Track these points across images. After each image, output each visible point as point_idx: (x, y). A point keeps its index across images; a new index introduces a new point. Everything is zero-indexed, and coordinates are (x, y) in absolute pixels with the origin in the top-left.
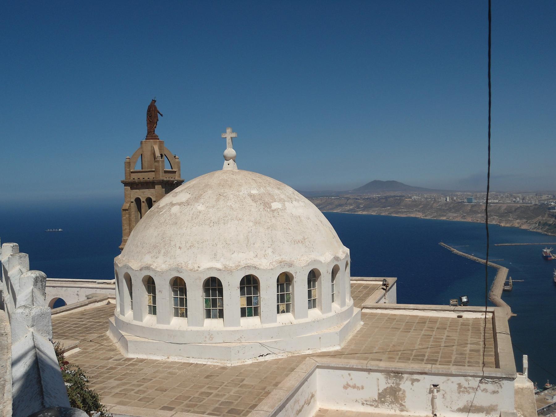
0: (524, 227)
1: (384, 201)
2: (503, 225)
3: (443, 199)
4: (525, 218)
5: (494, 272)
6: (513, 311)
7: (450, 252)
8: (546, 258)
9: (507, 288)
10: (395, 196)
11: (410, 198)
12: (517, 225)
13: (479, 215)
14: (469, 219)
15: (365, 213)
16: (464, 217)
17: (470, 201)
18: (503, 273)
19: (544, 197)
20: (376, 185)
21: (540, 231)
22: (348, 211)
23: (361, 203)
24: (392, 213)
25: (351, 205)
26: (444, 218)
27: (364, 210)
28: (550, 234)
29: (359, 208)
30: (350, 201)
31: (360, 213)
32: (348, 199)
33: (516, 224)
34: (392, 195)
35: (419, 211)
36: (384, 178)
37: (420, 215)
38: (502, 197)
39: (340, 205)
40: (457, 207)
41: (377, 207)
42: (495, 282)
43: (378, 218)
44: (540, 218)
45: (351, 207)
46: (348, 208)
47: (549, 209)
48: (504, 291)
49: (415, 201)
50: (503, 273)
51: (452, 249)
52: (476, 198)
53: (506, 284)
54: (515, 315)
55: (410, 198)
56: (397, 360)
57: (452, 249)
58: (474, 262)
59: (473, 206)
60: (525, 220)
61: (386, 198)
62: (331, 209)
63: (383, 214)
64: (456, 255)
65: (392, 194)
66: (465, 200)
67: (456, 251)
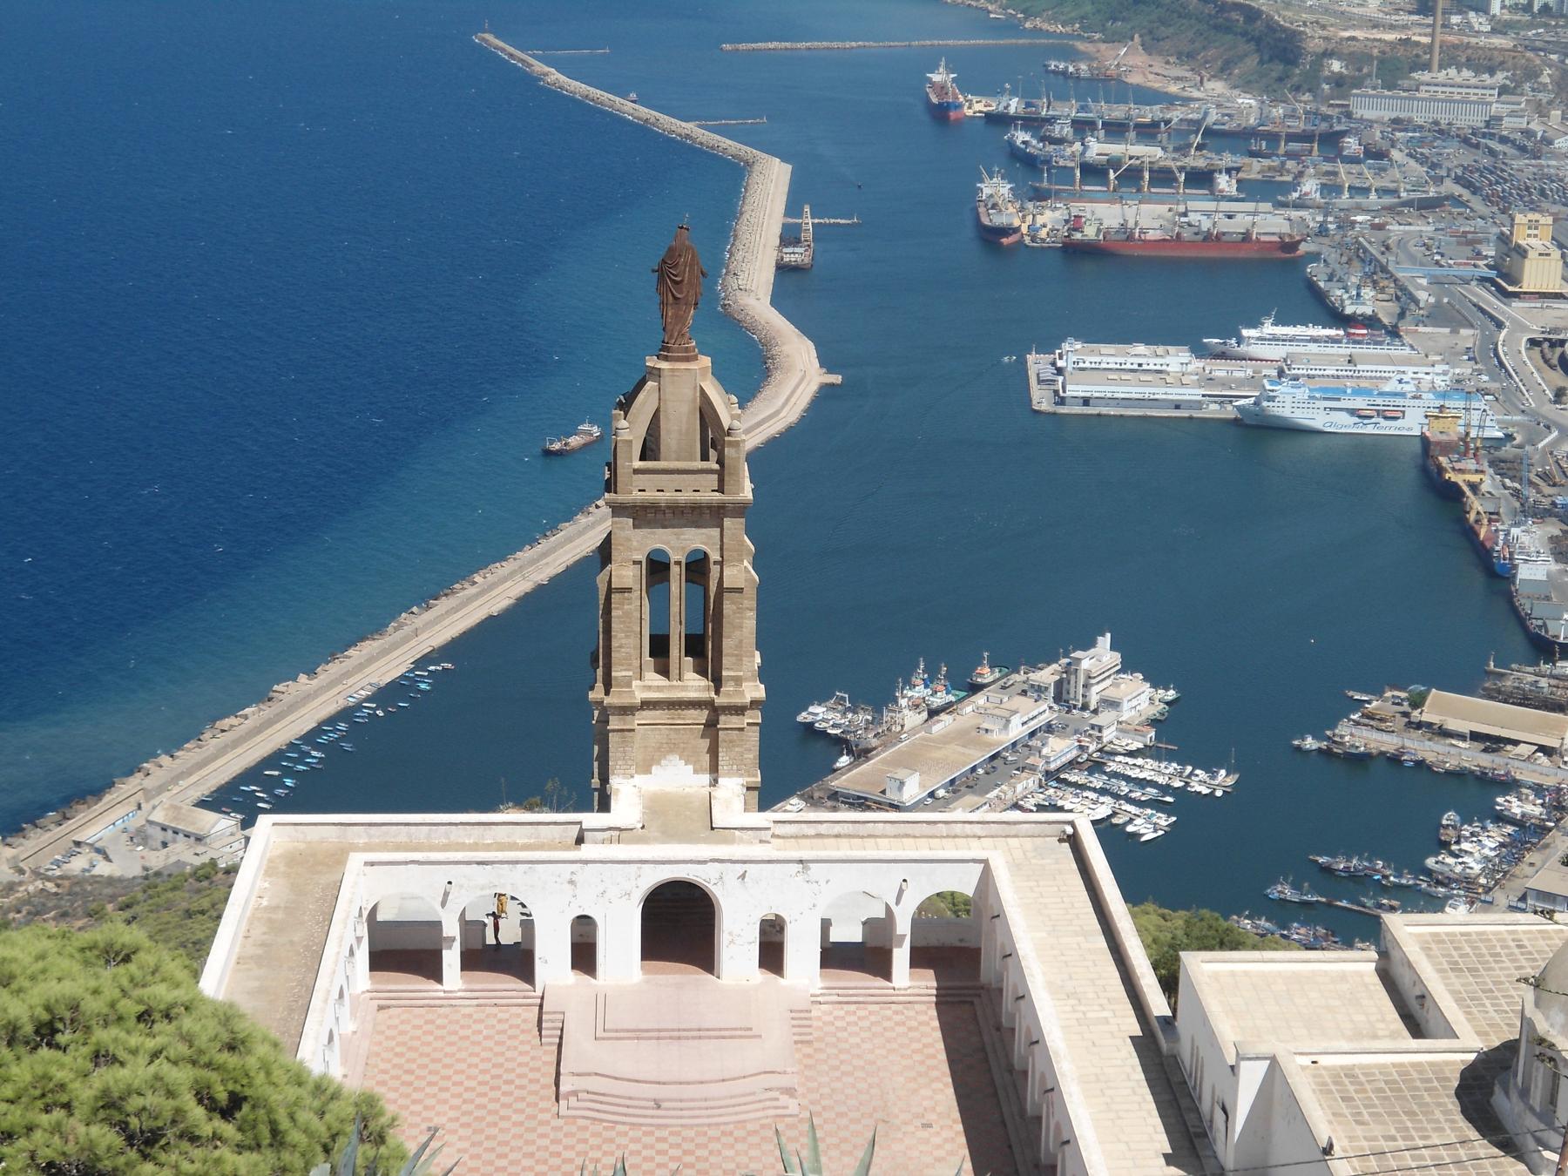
5: (734, 176)
6: (827, 363)
7: (531, 82)
9: (796, 255)
18: (771, 183)
42: (743, 228)
48: (783, 269)
51: (539, 67)
53: (789, 237)
54: (836, 379)
57: (539, 67)
58: (642, 131)
67: (555, 76)
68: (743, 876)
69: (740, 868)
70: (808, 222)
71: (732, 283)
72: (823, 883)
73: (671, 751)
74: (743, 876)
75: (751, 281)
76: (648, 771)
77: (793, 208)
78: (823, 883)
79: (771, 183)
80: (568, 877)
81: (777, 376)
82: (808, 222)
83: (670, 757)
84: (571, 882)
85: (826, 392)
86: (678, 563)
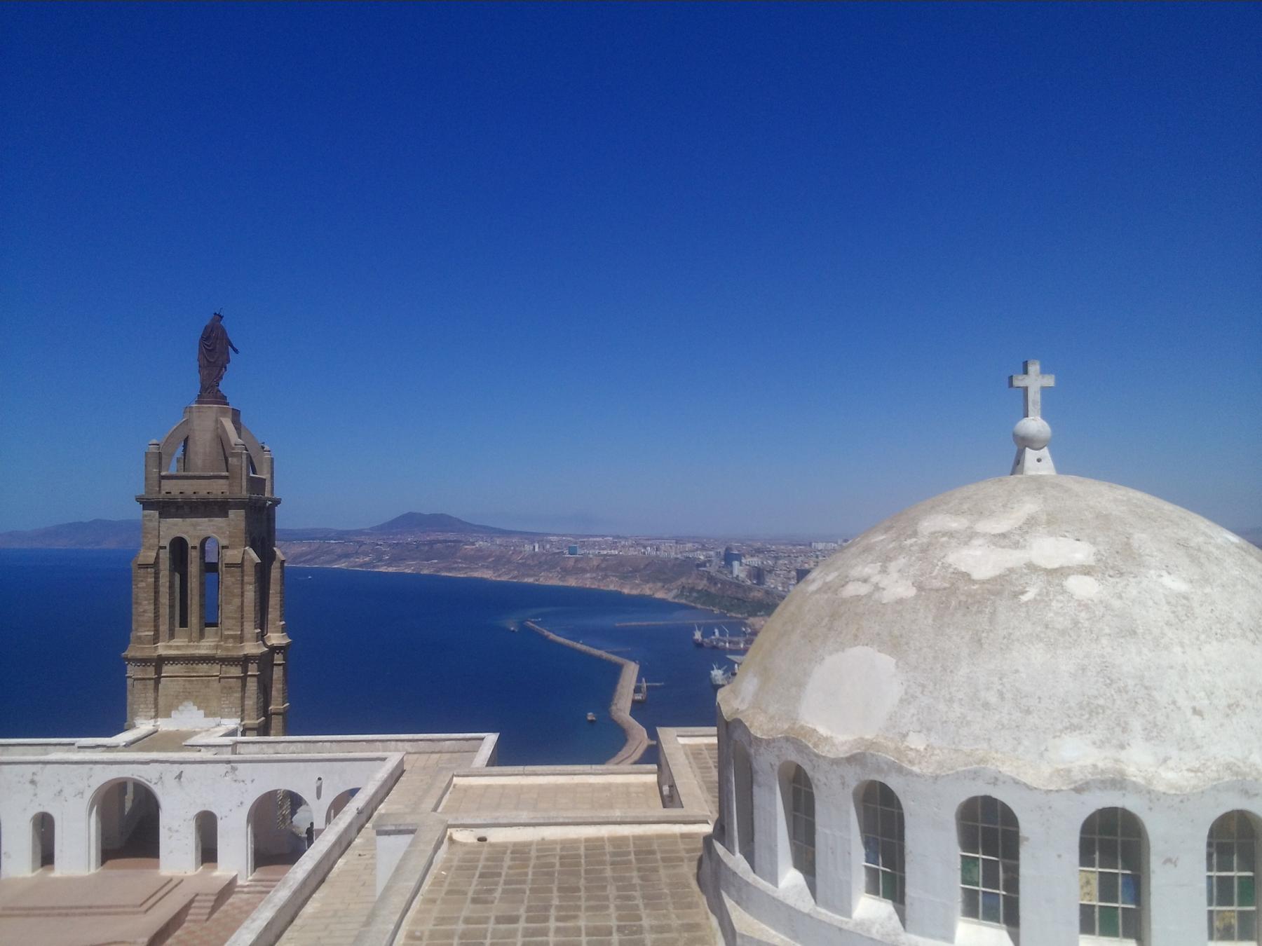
0: (660, 595)
1: (426, 548)
2: (626, 591)
3: (528, 548)
5: (616, 670)
7: (546, 637)
8: (699, 645)
9: (639, 697)
10: (445, 541)
11: (473, 544)
12: (648, 592)
14: (572, 582)
15: (391, 570)
16: (562, 578)
17: (573, 551)
18: (631, 672)
19: (689, 545)
20: (411, 521)
21: (683, 601)
22: (361, 566)
24: (441, 569)
25: (367, 554)
26: (531, 580)
27: (389, 565)
28: (699, 606)
29: (381, 560)
30: (363, 548)
31: (383, 569)
32: (361, 544)
33: (647, 590)
34: (441, 538)
35: (487, 567)
37: (488, 575)
39: (347, 556)
40: (550, 562)
41: (413, 559)
42: (619, 687)
43: (416, 577)
44: (683, 580)
46: (360, 560)
47: (699, 566)
48: (634, 702)
49: (480, 550)
50: (631, 672)
51: (546, 633)
53: (637, 690)
55: (473, 544)
56: (534, 847)
59: (577, 561)
60: (660, 584)
61: (432, 543)
63: (425, 572)
64: (552, 642)
66: (566, 551)
67: (552, 636)
71: (614, 708)
73: (186, 699)
76: (169, 716)
77: (639, 680)
80: (29, 777)
81: (630, 741)
83: (186, 703)
84: (33, 782)
86: (194, 548)
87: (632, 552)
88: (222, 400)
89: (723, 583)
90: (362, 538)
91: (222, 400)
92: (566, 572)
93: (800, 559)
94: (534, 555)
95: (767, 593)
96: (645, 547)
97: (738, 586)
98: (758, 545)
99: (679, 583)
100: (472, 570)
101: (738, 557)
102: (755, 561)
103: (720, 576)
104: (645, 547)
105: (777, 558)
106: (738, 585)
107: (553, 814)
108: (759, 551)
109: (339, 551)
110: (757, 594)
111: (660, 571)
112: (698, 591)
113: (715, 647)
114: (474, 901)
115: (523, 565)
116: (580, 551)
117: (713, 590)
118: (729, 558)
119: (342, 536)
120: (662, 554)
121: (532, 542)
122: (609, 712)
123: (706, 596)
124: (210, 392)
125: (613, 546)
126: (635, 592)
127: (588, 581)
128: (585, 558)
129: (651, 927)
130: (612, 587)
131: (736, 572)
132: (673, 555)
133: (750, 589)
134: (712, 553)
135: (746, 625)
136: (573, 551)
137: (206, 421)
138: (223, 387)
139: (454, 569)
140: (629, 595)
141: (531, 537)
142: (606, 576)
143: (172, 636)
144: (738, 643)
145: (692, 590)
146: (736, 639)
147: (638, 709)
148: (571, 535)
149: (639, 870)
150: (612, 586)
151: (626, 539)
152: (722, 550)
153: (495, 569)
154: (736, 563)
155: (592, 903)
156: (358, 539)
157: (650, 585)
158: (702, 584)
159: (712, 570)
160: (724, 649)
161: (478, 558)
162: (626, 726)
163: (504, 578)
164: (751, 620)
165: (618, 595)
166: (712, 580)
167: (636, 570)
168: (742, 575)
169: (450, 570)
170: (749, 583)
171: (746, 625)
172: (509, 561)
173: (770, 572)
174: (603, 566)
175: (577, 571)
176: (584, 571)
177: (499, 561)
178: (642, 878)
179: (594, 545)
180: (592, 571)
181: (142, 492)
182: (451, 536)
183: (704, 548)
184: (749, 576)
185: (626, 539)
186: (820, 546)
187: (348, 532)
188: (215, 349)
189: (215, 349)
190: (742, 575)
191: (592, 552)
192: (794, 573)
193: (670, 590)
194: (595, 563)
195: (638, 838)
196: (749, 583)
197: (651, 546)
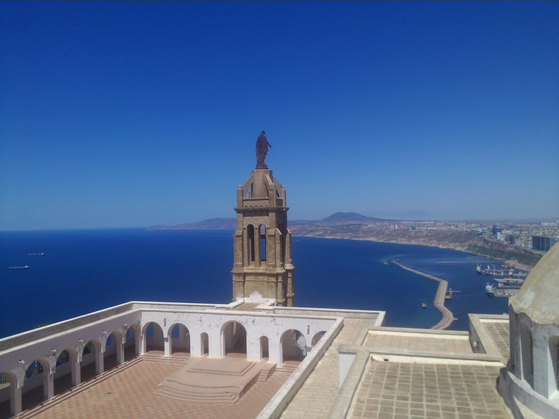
0: (458, 249)
1: (346, 228)
2: (441, 247)
4: (458, 241)
6: (455, 316)
7: (401, 268)
8: (479, 273)
9: (448, 297)
10: (354, 225)
11: (367, 225)
13: (422, 239)
14: (413, 242)
15: (331, 237)
16: (409, 241)
17: (414, 228)
18: (444, 286)
19: (473, 225)
20: (339, 216)
21: (470, 252)
22: (318, 236)
23: (328, 230)
24: (352, 237)
25: (320, 231)
26: (393, 242)
28: (479, 254)
30: (319, 228)
31: (327, 237)
32: (318, 226)
33: (451, 246)
35: (373, 236)
36: (345, 210)
37: (374, 239)
38: (439, 226)
39: (312, 231)
40: (404, 233)
41: (340, 233)
42: (438, 292)
43: (342, 241)
44: (471, 241)
45: (321, 233)
46: (318, 233)
47: (478, 235)
48: (446, 300)
49: (370, 228)
51: (401, 266)
52: (418, 226)
53: (447, 294)
54: (456, 319)
55: (367, 225)
58: (420, 276)
59: (416, 232)
60: (458, 244)
61: (348, 225)
62: (305, 234)
63: (346, 238)
64: (405, 270)
65: (352, 223)
67: (404, 267)
68: (254, 321)
69: (253, 318)
70: (451, 292)
71: (435, 302)
72: (280, 325)
74: (254, 321)
75: (440, 300)
77: (448, 289)
78: (280, 325)
79: (444, 286)
81: (444, 318)
82: (451, 292)
85: (454, 322)
86: (256, 229)
87: (444, 228)
88: (266, 167)
89: (492, 243)
90: (319, 224)
91: (266, 167)
92: (410, 238)
93: (534, 231)
94: (395, 230)
95: (516, 248)
96: (450, 226)
97: (500, 245)
98: (511, 224)
99: (468, 243)
100: (368, 237)
101: (500, 230)
102: (509, 232)
103: (490, 240)
104: (450, 226)
105: (521, 231)
106: (500, 244)
107: (420, 351)
108: (511, 227)
109: (309, 229)
110: (510, 249)
111: (458, 237)
112: (479, 247)
113: (488, 275)
114: (386, 388)
115: (390, 235)
116: (417, 228)
117: (486, 246)
118: (495, 231)
119: (310, 223)
120: (459, 229)
121: (394, 224)
122: (433, 303)
123: (483, 250)
124: (261, 165)
125: (434, 225)
126: (445, 247)
127: (421, 242)
128: (420, 231)
129: (475, 410)
130: (433, 245)
131: (499, 238)
132: (465, 229)
133: (507, 246)
134: (486, 228)
135: (504, 264)
136: (414, 228)
137: (260, 176)
138: (266, 162)
139: (358, 237)
140: (442, 249)
141: (393, 222)
142: (430, 240)
143: (249, 265)
144: (500, 273)
145: (475, 246)
146: (499, 271)
147: (447, 303)
148: (412, 221)
149: (466, 381)
150: (434, 244)
151: (440, 222)
152: (491, 227)
153: (377, 237)
154: (499, 234)
155: (444, 395)
156: (317, 224)
157: (453, 244)
158: (481, 244)
159: (486, 236)
160: (493, 276)
161: (369, 232)
162: (442, 311)
163: (381, 241)
164: (507, 262)
165: (437, 249)
166: (486, 242)
167: (446, 237)
168: (502, 239)
169: (357, 237)
170: (506, 243)
171: (504, 264)
172: (383, 233)
173: (518, 237)
174: (429, 235)
175: (416, 237)
176: (419, 237)
177: (378, 233)
178: (467, 386)
179: (424, 225)
180: (423, 237)
181: (236, 207)
182: (357, 222)
183: (481, 226)
184: (506, 240)
185: (440, 222)
186: (546, 224)
187: (312, 221)
188: (262, 146)
189: (262, 146)
190: (502, 239)
191: (423, 229)
192: (531, 238)
193: (463, 246)
194: (425, 233)
195: (463, 366)
196: (506, 243)
197: (453, 225)
